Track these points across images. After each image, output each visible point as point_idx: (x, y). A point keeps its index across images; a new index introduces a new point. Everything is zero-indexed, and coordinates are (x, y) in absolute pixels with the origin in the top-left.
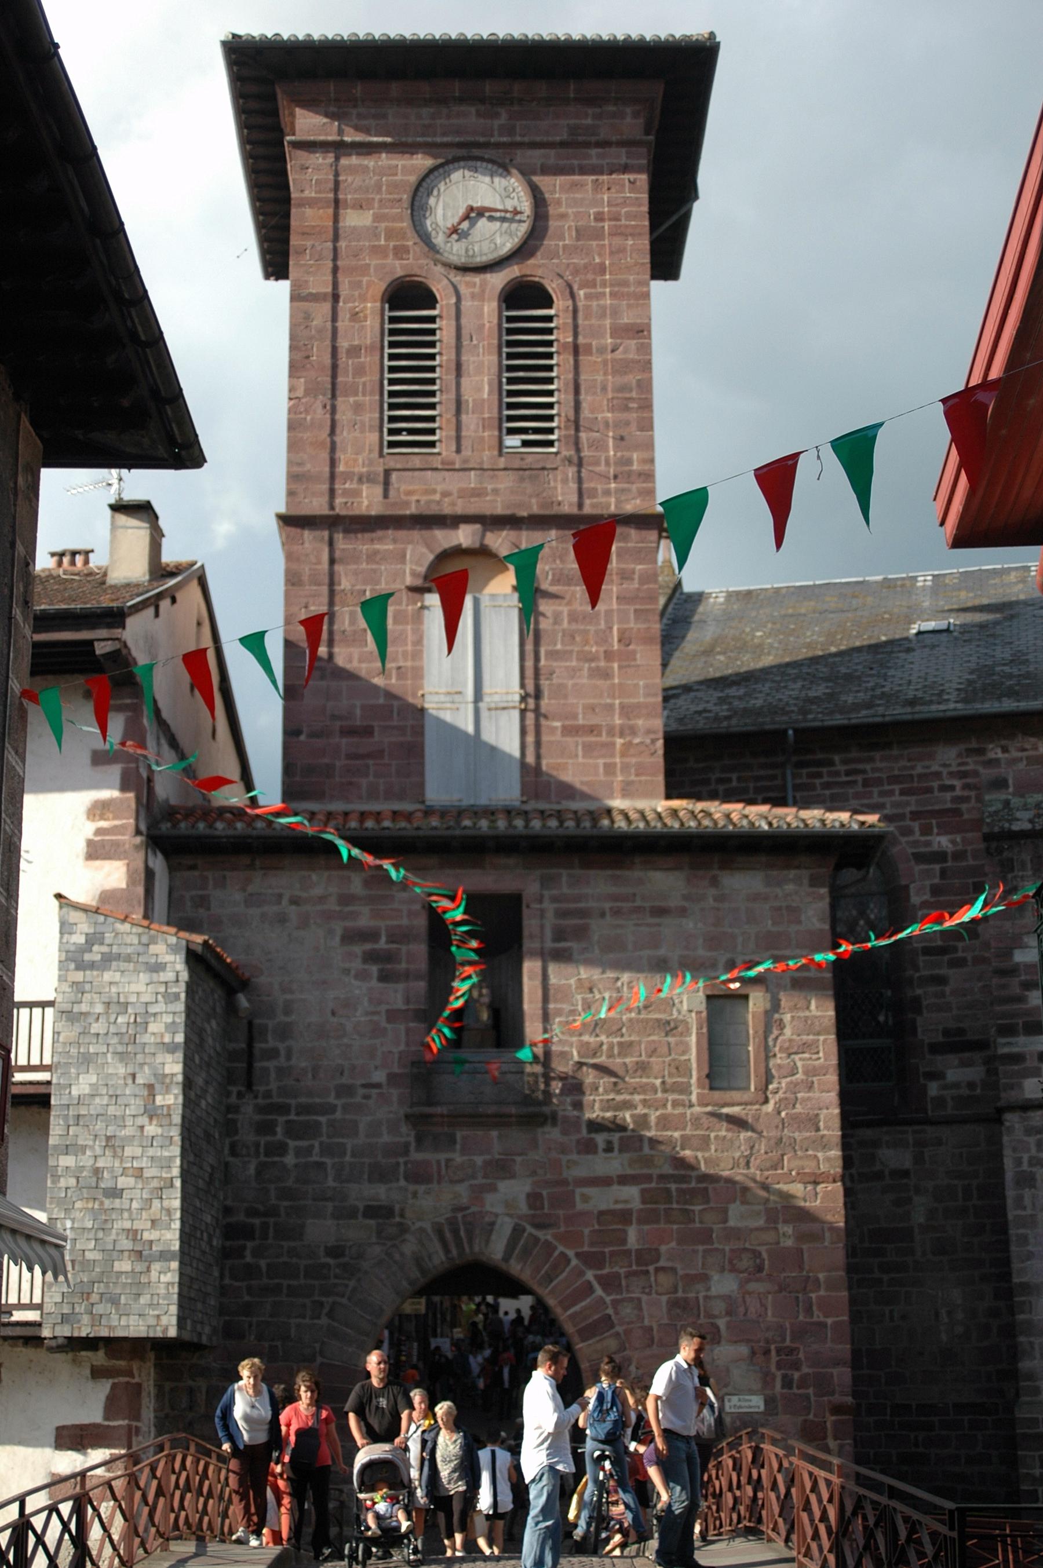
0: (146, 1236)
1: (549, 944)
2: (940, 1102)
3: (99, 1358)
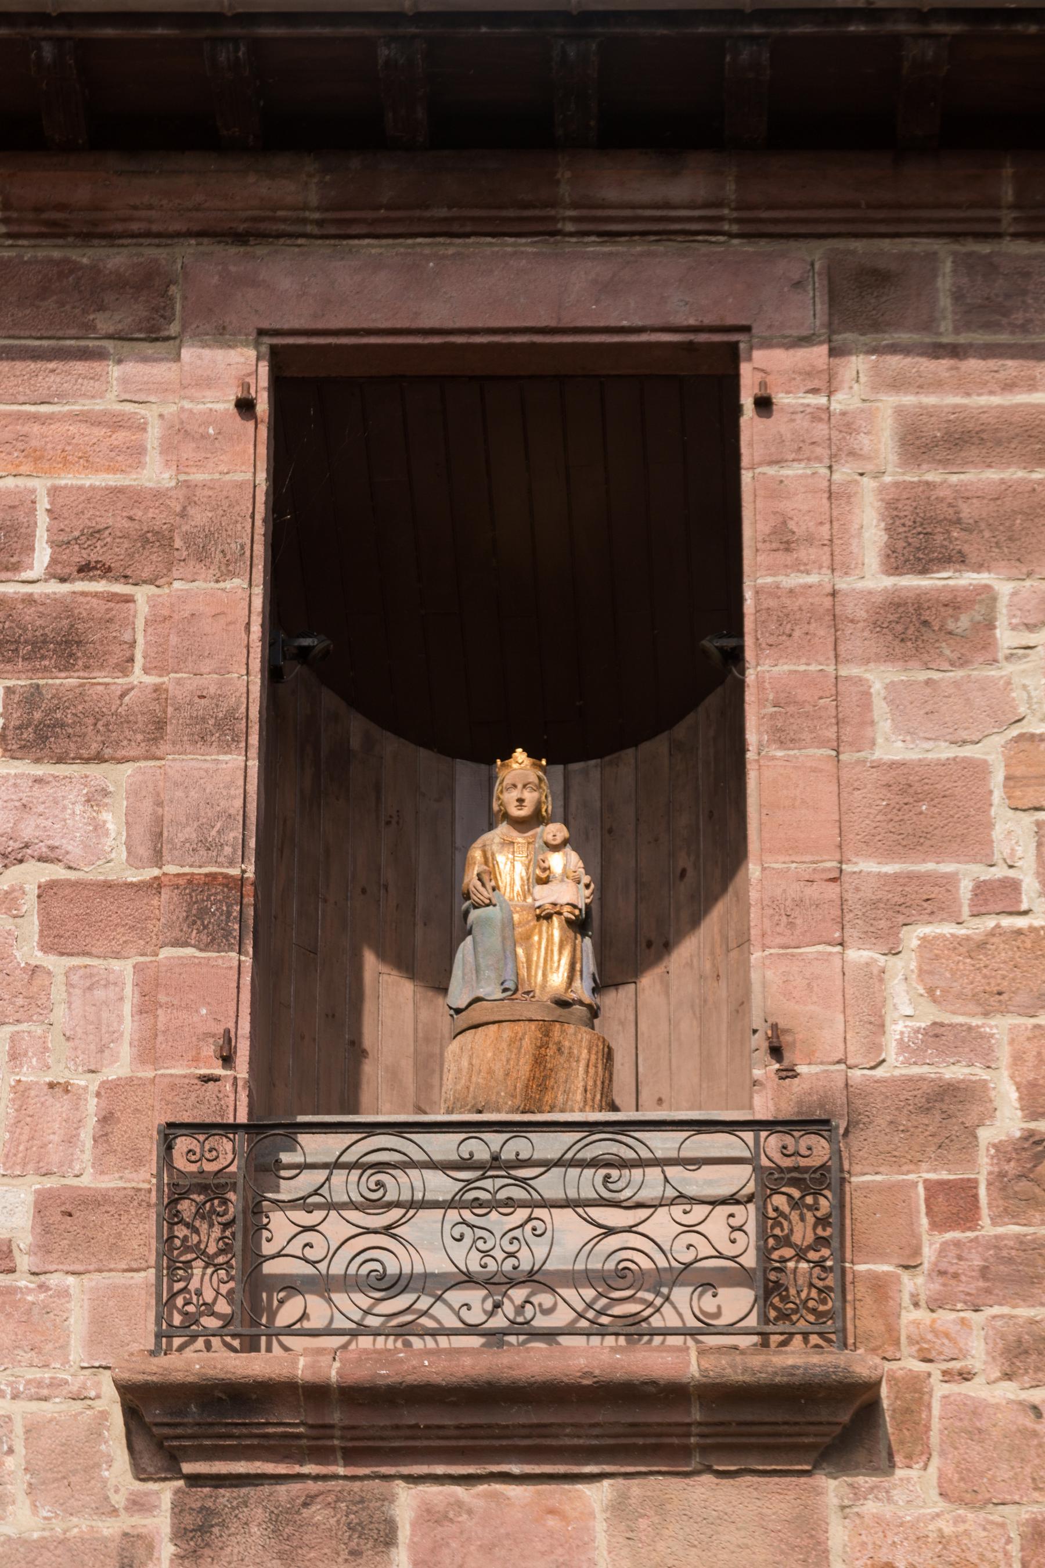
1: (871, 578)
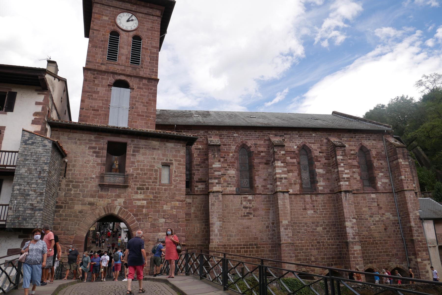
0: (35, 205)
1: (132, 153)
2: (197, 191)
3: (21, 233)
